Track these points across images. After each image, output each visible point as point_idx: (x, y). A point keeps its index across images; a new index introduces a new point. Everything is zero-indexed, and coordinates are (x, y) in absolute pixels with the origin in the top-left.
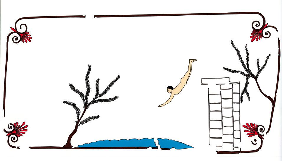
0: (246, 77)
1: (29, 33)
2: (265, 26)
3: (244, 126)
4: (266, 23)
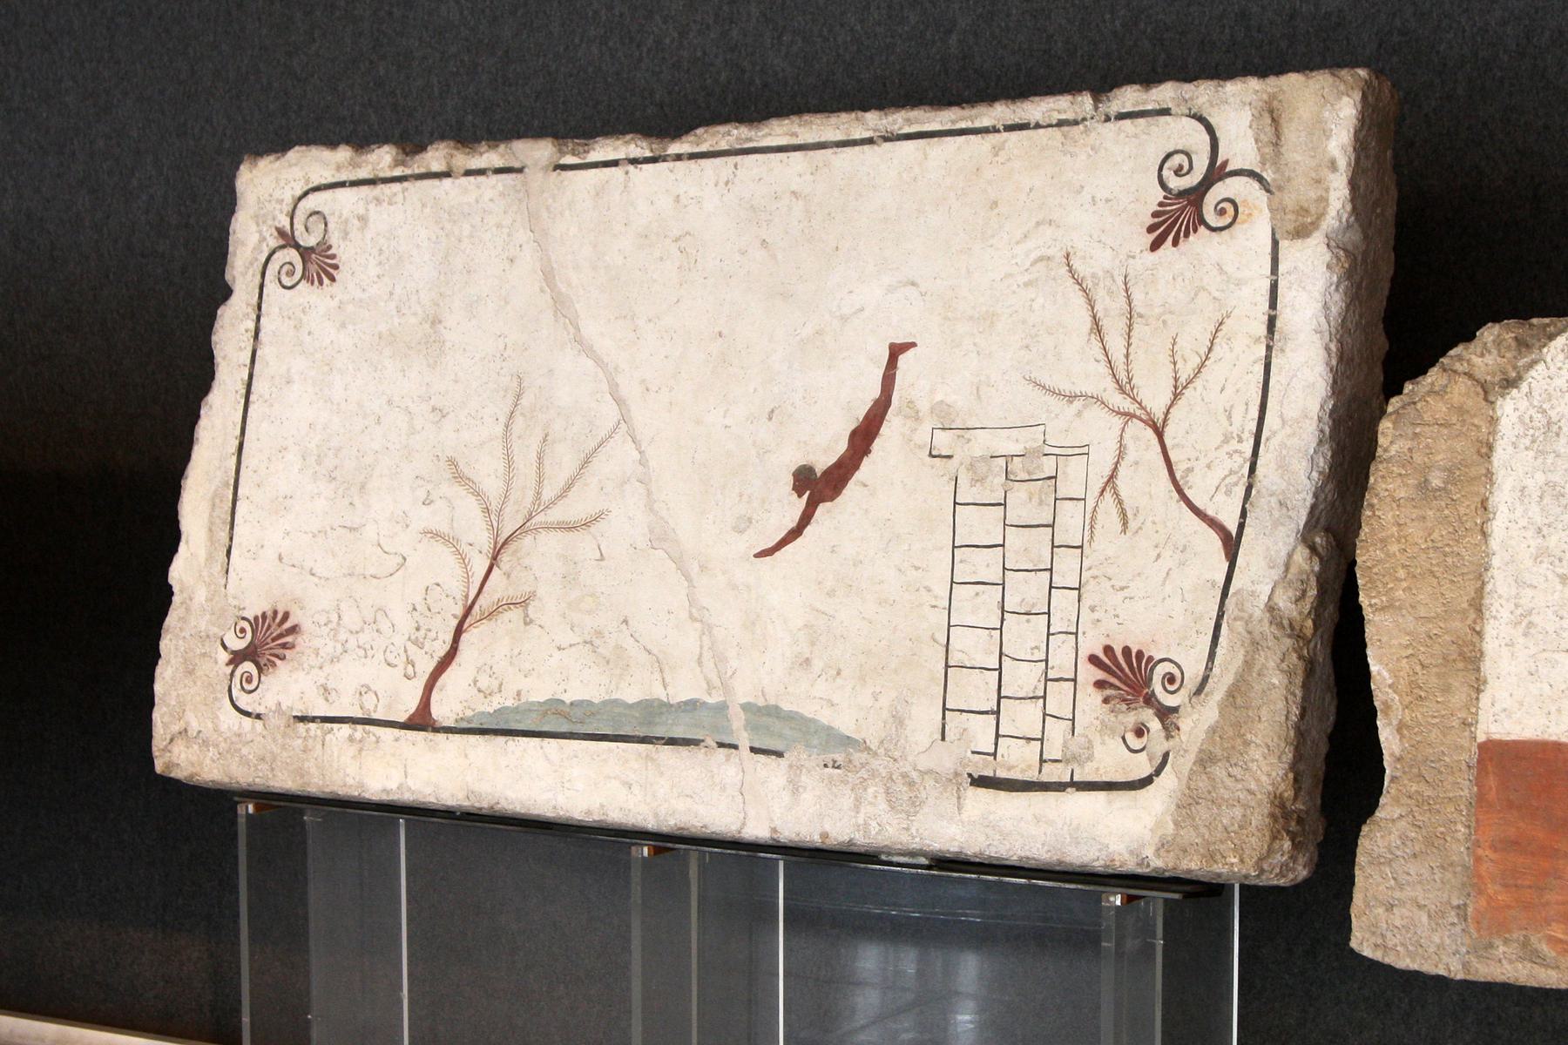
0: (1118, 422)
1: (330, 247)
2: (1217, 173)
3: (1093, 659)
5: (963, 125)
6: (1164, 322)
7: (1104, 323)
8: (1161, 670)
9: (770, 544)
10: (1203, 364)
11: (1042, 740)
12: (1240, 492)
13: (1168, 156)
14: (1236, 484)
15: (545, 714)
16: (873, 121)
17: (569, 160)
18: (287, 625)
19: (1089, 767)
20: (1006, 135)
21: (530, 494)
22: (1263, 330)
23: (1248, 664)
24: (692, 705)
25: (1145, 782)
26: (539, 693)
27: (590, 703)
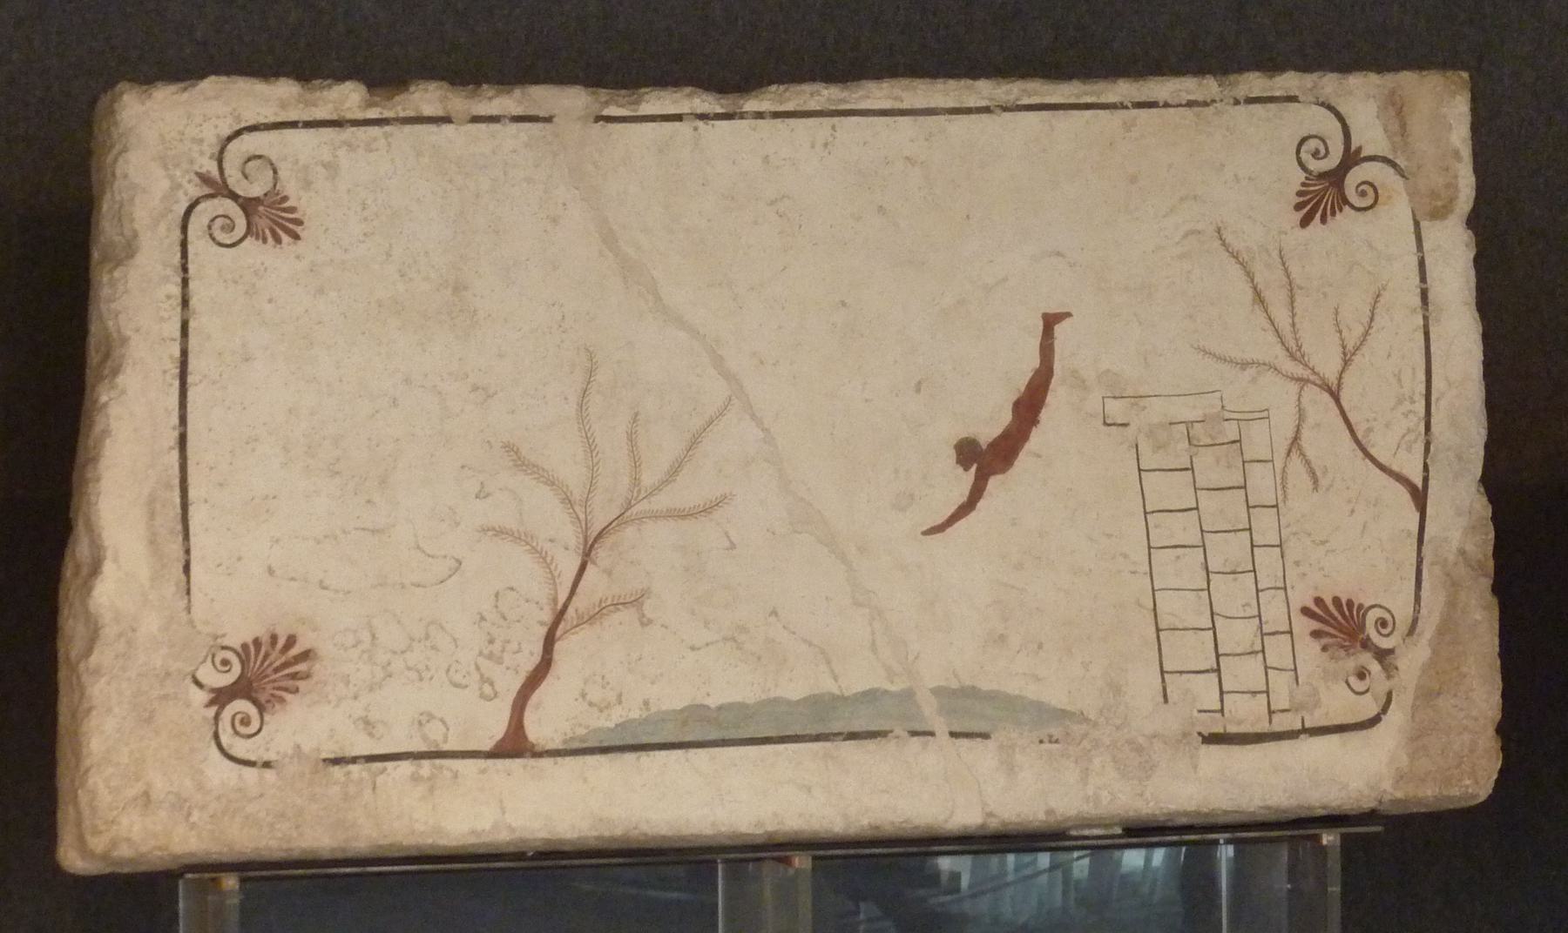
0: (1293, 388)
1: (285, 199)
2: (1352, 158)
3: (1306, 611)
4: (1353, 148)
5: (1089, 100)
6: (1325, 294)
7: (1266, 294)
8: (1372, 617)
9: (940, 521)
10: (1366, 333)
11: (1267, 692)
12: (1420, 447)
13: (1303, 141)
14: (1415, 441)
15: (685, 723)
16: (984, 90)
17: (613, 111)
18: (294, 651)
19: (1318, 713)
20: (1136, 111)
21: (626, 480)
22: (1417, 301)
23: (1451, 604)
24: (871, 696)
25: (1374, 721)
26: (673, 697)
27: (742, 706)
